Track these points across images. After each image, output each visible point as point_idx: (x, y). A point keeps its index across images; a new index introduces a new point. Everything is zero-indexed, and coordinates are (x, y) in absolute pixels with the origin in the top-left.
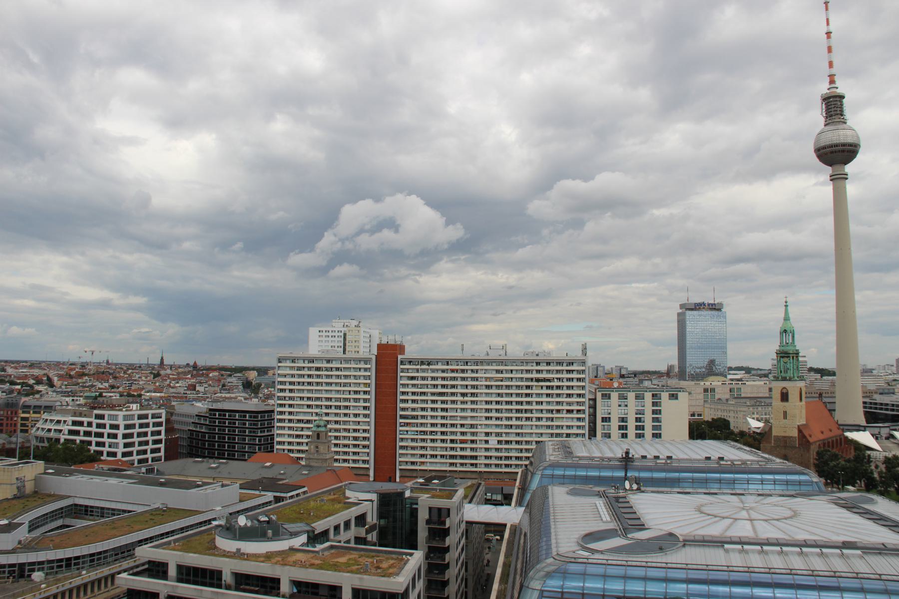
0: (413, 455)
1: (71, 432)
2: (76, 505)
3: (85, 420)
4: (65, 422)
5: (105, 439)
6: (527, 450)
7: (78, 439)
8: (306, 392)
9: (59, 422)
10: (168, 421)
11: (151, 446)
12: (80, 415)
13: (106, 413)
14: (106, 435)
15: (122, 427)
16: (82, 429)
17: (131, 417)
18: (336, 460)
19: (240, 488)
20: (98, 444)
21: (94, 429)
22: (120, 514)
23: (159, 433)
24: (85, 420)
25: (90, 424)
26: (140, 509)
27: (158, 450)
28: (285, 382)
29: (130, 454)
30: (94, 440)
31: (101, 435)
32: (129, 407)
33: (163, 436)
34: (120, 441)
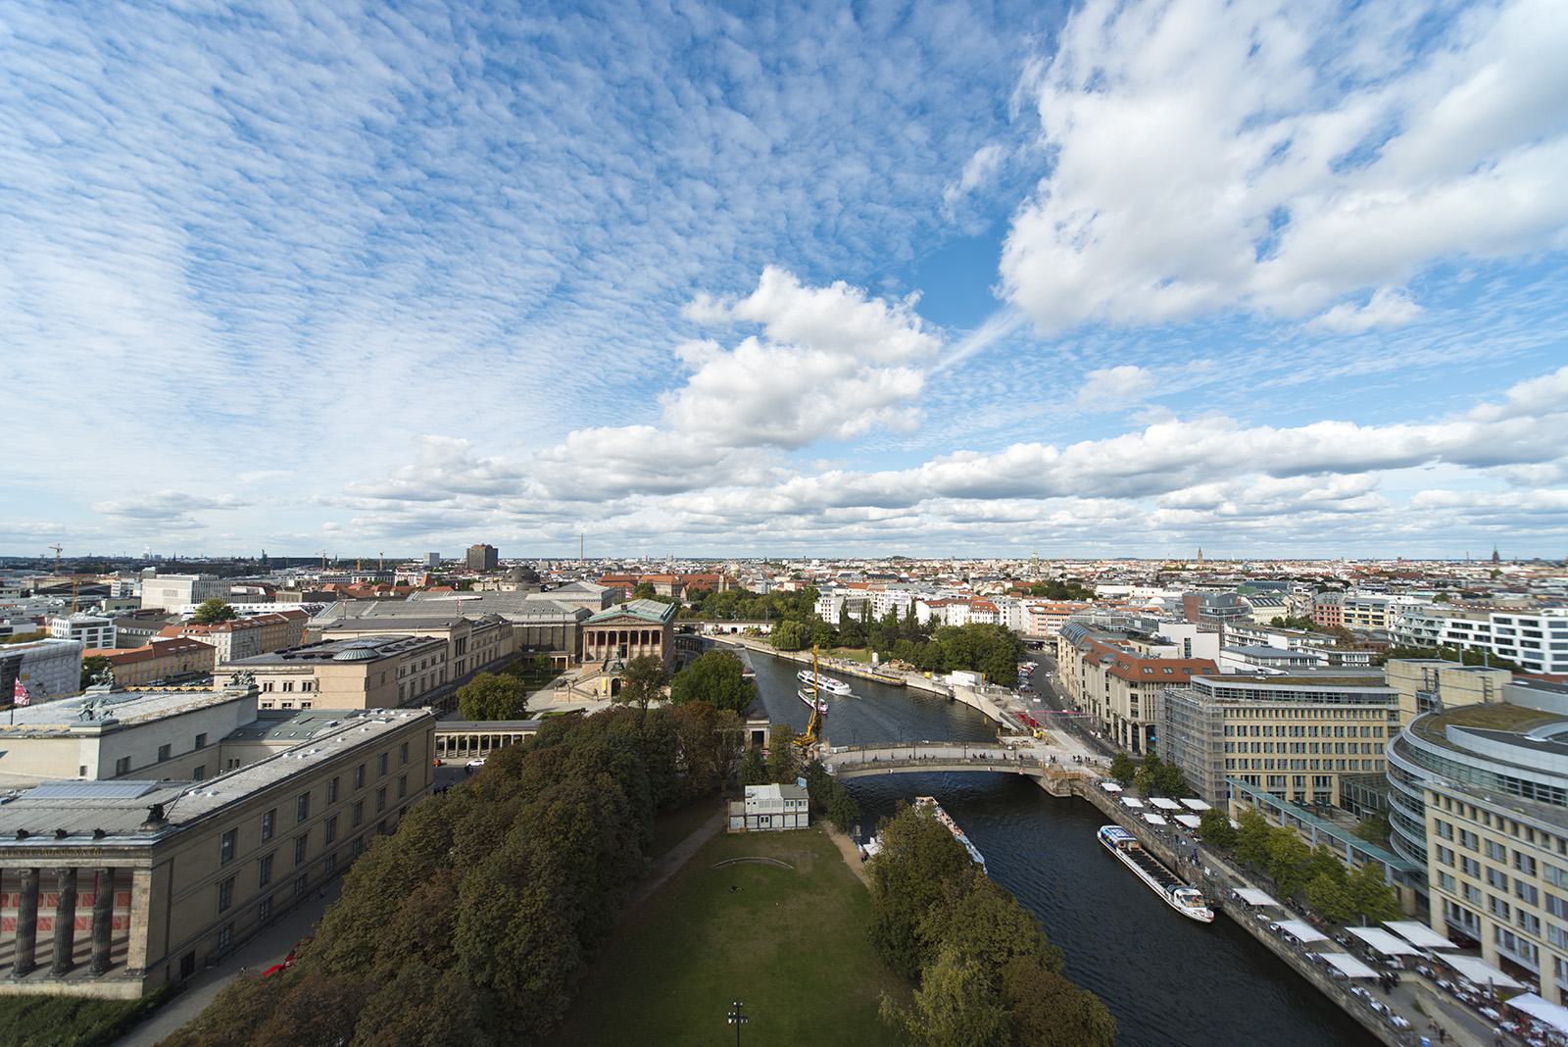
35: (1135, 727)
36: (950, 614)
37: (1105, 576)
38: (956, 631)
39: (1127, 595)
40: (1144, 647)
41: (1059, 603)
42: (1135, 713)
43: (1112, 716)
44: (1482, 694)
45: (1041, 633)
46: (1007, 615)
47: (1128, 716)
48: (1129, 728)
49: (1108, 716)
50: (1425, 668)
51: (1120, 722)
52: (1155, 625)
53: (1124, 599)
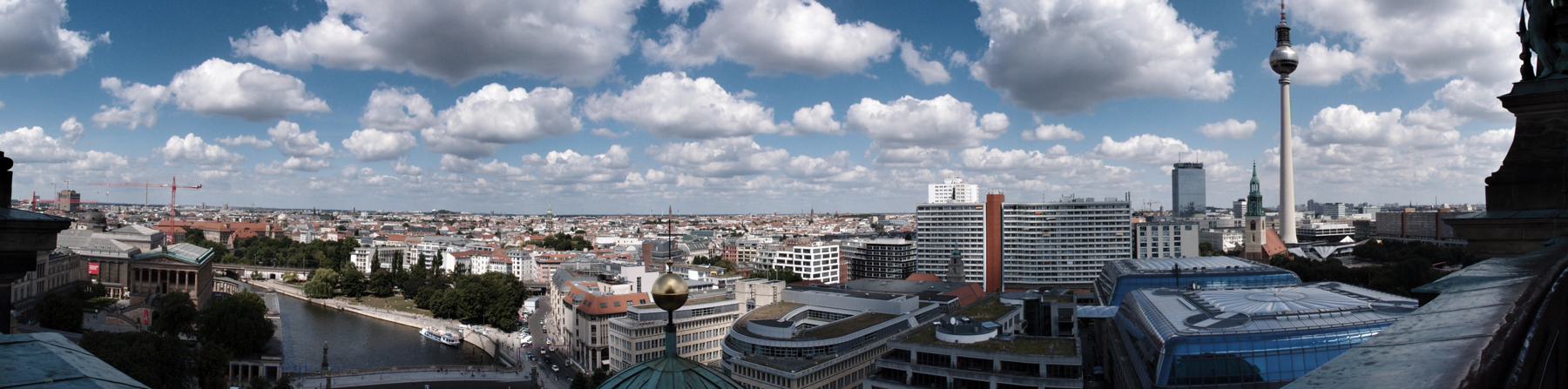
0: (1014, 273)
1: (779, 261)
3: (788, 253)
5: (802, 266)
6: (1098, 268)
12: (784, 250)
13: (802, 248)
16: (786, 259)
17: (817, 251)
18: (968, 278)
24: (788, 253)
25: (791, 256)
26: (856, 314)
27: (835, 273)
30: (794, 266)
31: (799, 263)
33: (838, 264)
34: (812, 267)
35: (594, 351)
36: (474, 264)
37: (605, 229)
38: (477, 278)
39: (614, 244)
40: (607, 286)
41: (559, 253)
42: (594, 340)
43: (580, 345)
44: (772, 297)
45: (544, 280)
46: (520, 265)
47: (590, 344)
48: (590, 352)
49: (578, 345)
50: (751, 285)
51: (585, 349)
52: (617, 268)
53: (612, 247)
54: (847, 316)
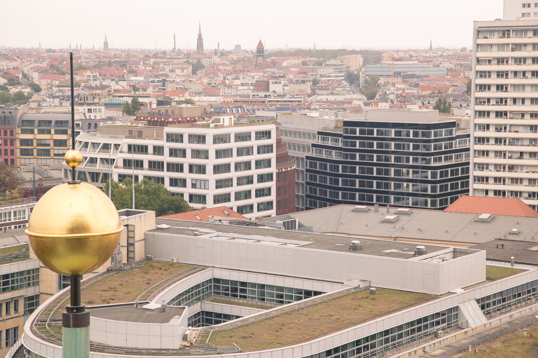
2: (217, 280)
4: (117, 146)
7: (141, 173)
8: (528, 89)
9: (106, 147)
10: (279, 142)
11: (256, 185)
12: (140, 135)
13: (186, 131)
14: (186, 168)
15: (212, 154)
16: (145, 158)
19: (487, 259)
20: (174, 182)
21: (166, 158)
22: (301, 298)
23: (268, 163)
25: (158, 150)
26: (330, 290)
28: (489, 72)
29: (226, 198)
30: (167, 175)
31: (179, 168)
32: (219, 120)
33: (273, 169)
54: (308, 294)
